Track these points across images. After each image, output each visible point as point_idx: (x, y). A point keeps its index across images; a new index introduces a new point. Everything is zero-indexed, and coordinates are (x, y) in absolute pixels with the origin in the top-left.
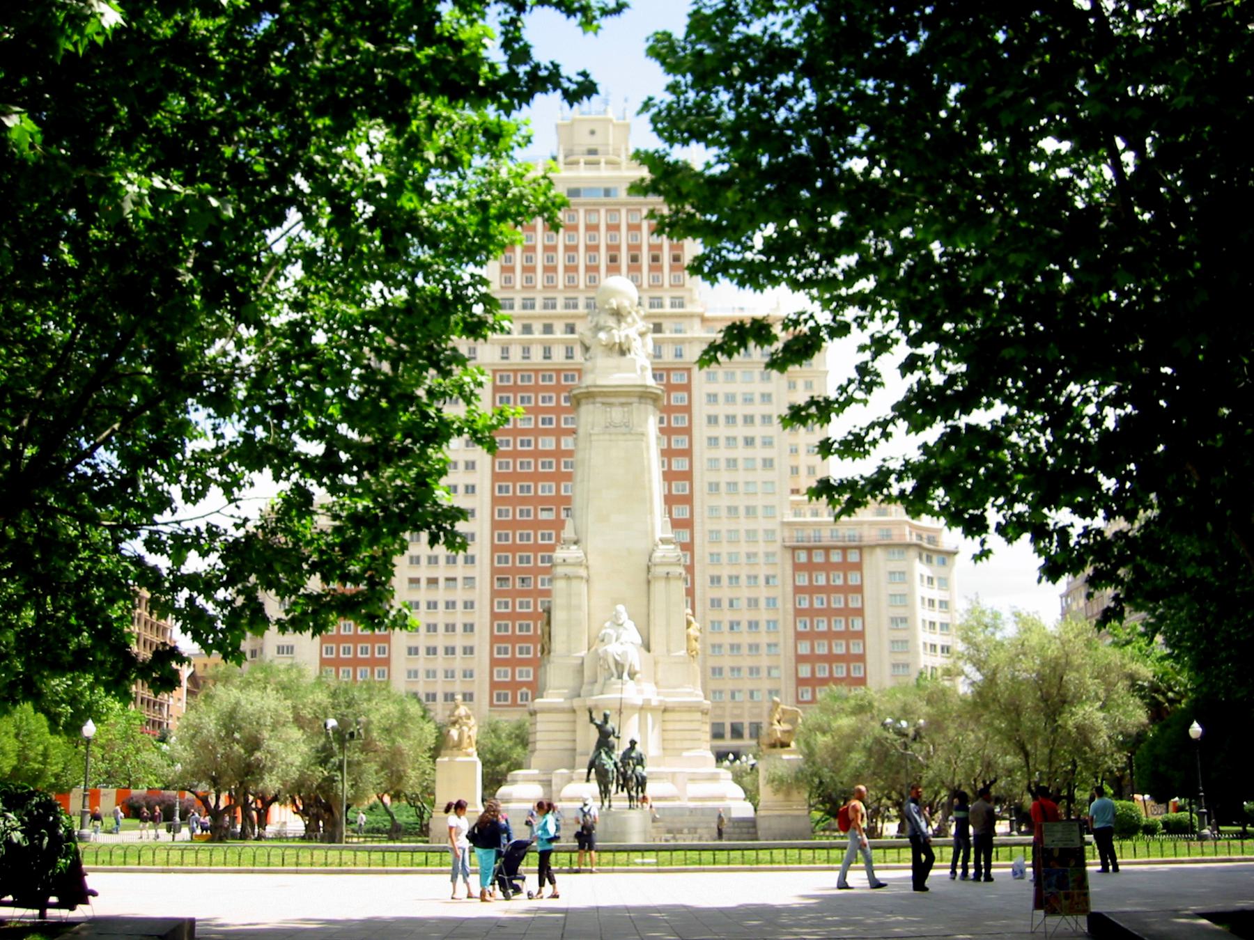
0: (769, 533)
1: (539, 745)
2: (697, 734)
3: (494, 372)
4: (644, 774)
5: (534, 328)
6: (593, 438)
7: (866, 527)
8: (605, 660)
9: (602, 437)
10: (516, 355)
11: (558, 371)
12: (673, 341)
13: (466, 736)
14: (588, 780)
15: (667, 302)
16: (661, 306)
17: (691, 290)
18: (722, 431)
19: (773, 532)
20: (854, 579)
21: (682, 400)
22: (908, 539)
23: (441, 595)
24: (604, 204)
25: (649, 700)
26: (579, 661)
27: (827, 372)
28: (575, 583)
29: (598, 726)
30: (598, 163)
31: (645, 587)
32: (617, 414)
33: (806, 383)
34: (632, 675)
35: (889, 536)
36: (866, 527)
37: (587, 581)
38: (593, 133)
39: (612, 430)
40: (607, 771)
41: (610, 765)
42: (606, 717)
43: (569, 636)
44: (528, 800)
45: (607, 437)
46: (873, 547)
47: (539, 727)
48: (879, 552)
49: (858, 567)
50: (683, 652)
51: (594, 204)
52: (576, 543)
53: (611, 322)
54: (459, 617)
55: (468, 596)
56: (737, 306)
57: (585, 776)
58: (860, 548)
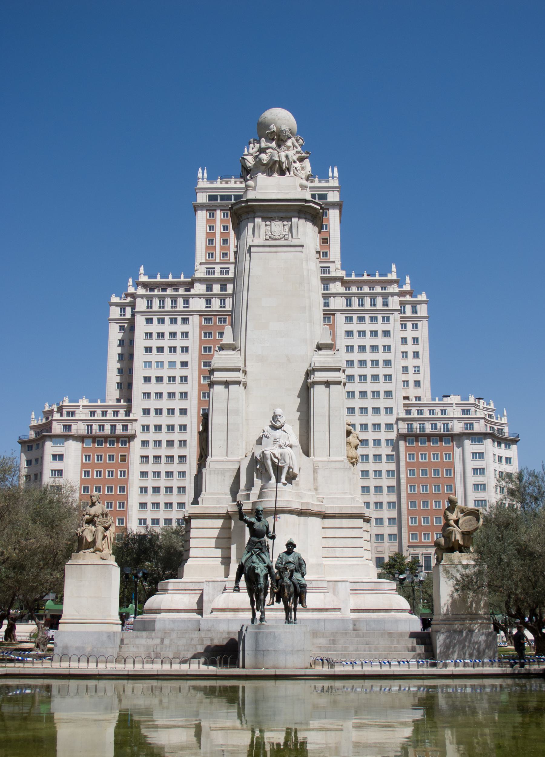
0: (389, 427)
1: (193, 552)
2: (359, 542)
4: (304, 583)
5: (228, 287)
6: (253, 249)
7: (455, 422)
10: (216, 304)
13: (100, 536)
14: (237, 589)
19: (392, 425)
22: (483, 430)
23: (163, 467)
29: (251, 525)
33: (413, 324)
37: (245, 385)
40: (258, 575)
41: (261, 570)
44: (178, 611)
50: (344, 458)
54: (175, 483)
55: (182, 468)
57: (233, 585)
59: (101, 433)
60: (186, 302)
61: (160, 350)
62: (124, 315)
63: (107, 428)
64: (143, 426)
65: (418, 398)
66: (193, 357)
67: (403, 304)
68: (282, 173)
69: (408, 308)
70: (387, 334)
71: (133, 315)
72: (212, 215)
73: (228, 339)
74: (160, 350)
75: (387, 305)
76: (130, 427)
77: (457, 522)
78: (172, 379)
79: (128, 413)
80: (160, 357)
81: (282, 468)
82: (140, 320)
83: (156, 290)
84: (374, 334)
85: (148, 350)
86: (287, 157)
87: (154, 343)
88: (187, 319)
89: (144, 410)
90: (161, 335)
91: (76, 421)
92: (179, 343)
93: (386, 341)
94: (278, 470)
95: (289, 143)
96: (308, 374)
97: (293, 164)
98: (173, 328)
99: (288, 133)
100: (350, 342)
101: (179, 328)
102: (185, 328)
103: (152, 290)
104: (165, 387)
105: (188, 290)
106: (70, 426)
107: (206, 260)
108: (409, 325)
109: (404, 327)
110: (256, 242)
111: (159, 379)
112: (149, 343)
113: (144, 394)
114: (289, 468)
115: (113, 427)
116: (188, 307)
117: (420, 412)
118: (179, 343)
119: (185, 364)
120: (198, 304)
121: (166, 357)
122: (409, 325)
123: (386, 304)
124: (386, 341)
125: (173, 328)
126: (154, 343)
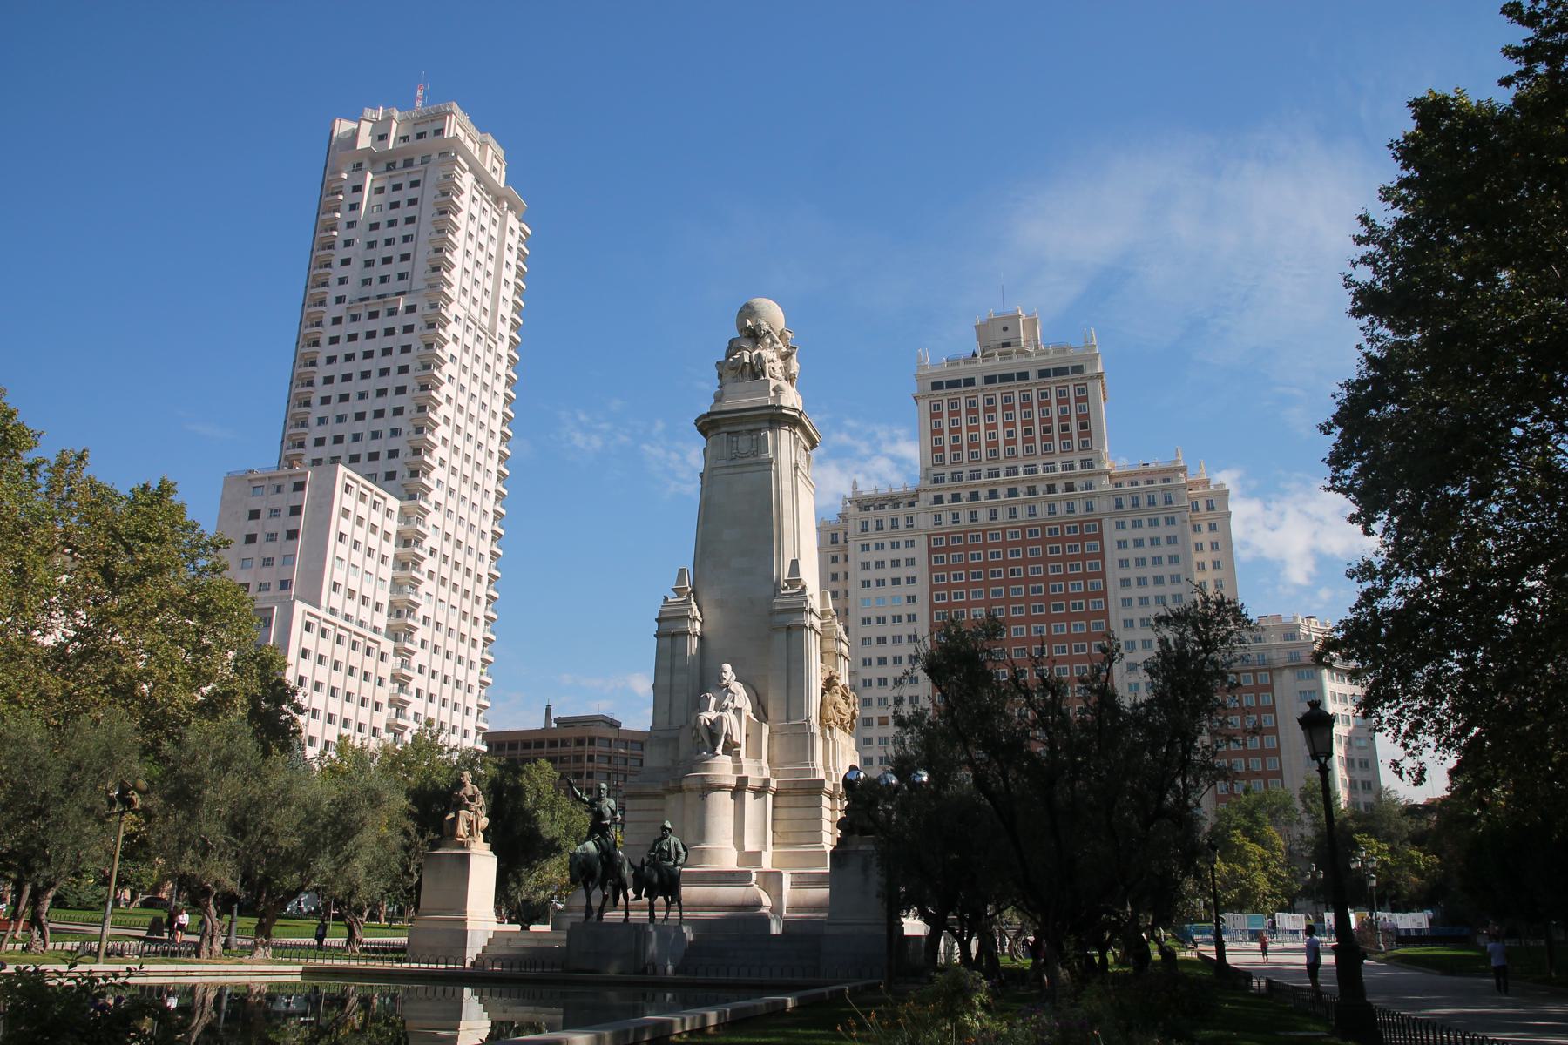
3: (929, 536)
5: (962, 496)
6: (715, 472)
7: (1274, 652)
8: (698, 730)
9: (725, 471)
10: (947, 519)
11: (984, 532)
12: (1083, 497)
15: (1078, 464)
16: (1073, 468)
17: (1098, 452)
18: (1133, 573)
20: (1265, 700)
21: (1095, 547)
24: (1018, 386)
25: (746, 778)
28: (679, 640)
30: (1010, 353)
32: (744, 443)
33: (1210, 525)
34: (730, 748)
36: (1274, 652)
38: (1005, 329)
39: (739, 462)
43: (670, 705)
45: (732, 470)
46: (1281, 669)
48: (1287, 672)
49: (1270, 688)
56: (1141, 462)
58: (1270, 671)
60: (910, 520)
61: (881, 583)
62: (837, 542)
64: (864, 681)
66: (921, 589)
70: (1172, 540)
71: (846, 541)
72: (937, 407)
74: (881, 583)
75: (1171, 502)
78: (897, 619)
80: (881, 591)
82: (853, 548)
83: (872, 508)
84: (1155, 542)
85: (866, 584)
86: (759, 355)
87: (873, 574)
88: (912, 541)
89: (864, 661)
90: (880, 564)
92: (903, 572)
93: (1172, 550)
97: (772, 364)
98: (895, 554)
99: (766, 327)
100: (1123, 554)
101: (903, 553)
102: (910, 553)
103: (867, 508)
104: (888, 630)
105: (911, 504)
107: (933, 465)
108: (1205, 527)
109: (1197, 529)
111: (881, 620)
112: (865, 575)
113: (864, 639)
114: (727, 735)
116: (912, 526)
118: (903, 572)
119: (911, 599)
120: (924, 521)
121: (889, 589)
122: (1205, 527)
123: (1168, 501)
124: (1172, 550)
125: (895, 554)
126: (873, 574)
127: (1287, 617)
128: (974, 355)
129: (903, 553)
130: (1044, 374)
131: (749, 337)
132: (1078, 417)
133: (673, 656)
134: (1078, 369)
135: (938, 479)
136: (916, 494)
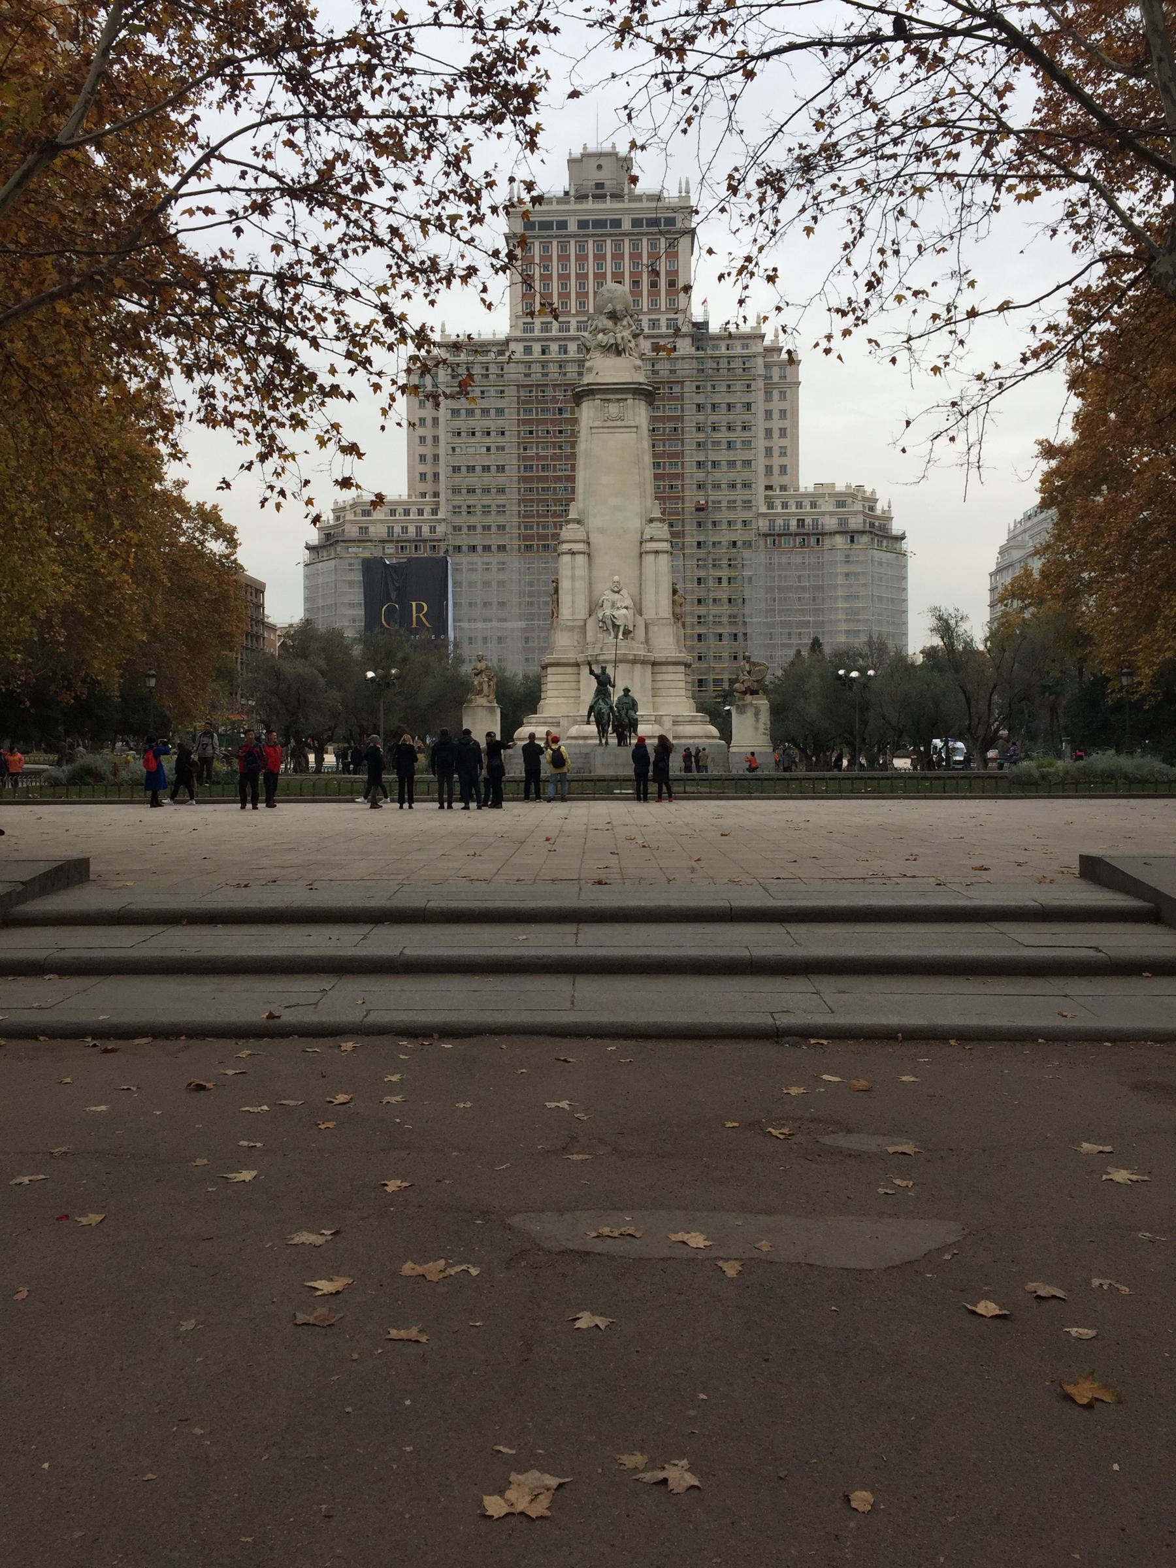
1: (549, 693)
6: (594, 431)
7: (827, 517)
9: (601, 430)
26: (582, 623)
27: (799, 383)
29: (597, 677)
30: (604, 196)
31: (637, 560)
32: (613, 409)
35: (846, 524)
36: (827, 517)
38: (599, 167)
42: (604, 669)
47: (549, 678)
51: (602, 235)
52: (579, 522)
53: (609, 324)
59: (404, 537)
63: (412, 530)
65: (783, 488)
67: (767, 366)
68: (619, 353)
69: (776, 373)
73: (573, 515)
76: (438, 529)
77: (749, 672)
79: (435, 512)
81: (619, 626)
91: (375, 522)
94: (616, 627)
95: (625, 323)
96: (641, 543)
102: (500, 404)
106: (367, 528)
110: (597, 424)
115: (419, 529)
117: (785, 505)
122: (776, 394)
127: (840, 487)
128: (566, 193)
129: (491, 403)
130: (636, 223)
131: (610, 318)
132: (668, 273)
133: (573, 568)
134: (671, 221)
135: (528, 328)
136: (507, 341)
